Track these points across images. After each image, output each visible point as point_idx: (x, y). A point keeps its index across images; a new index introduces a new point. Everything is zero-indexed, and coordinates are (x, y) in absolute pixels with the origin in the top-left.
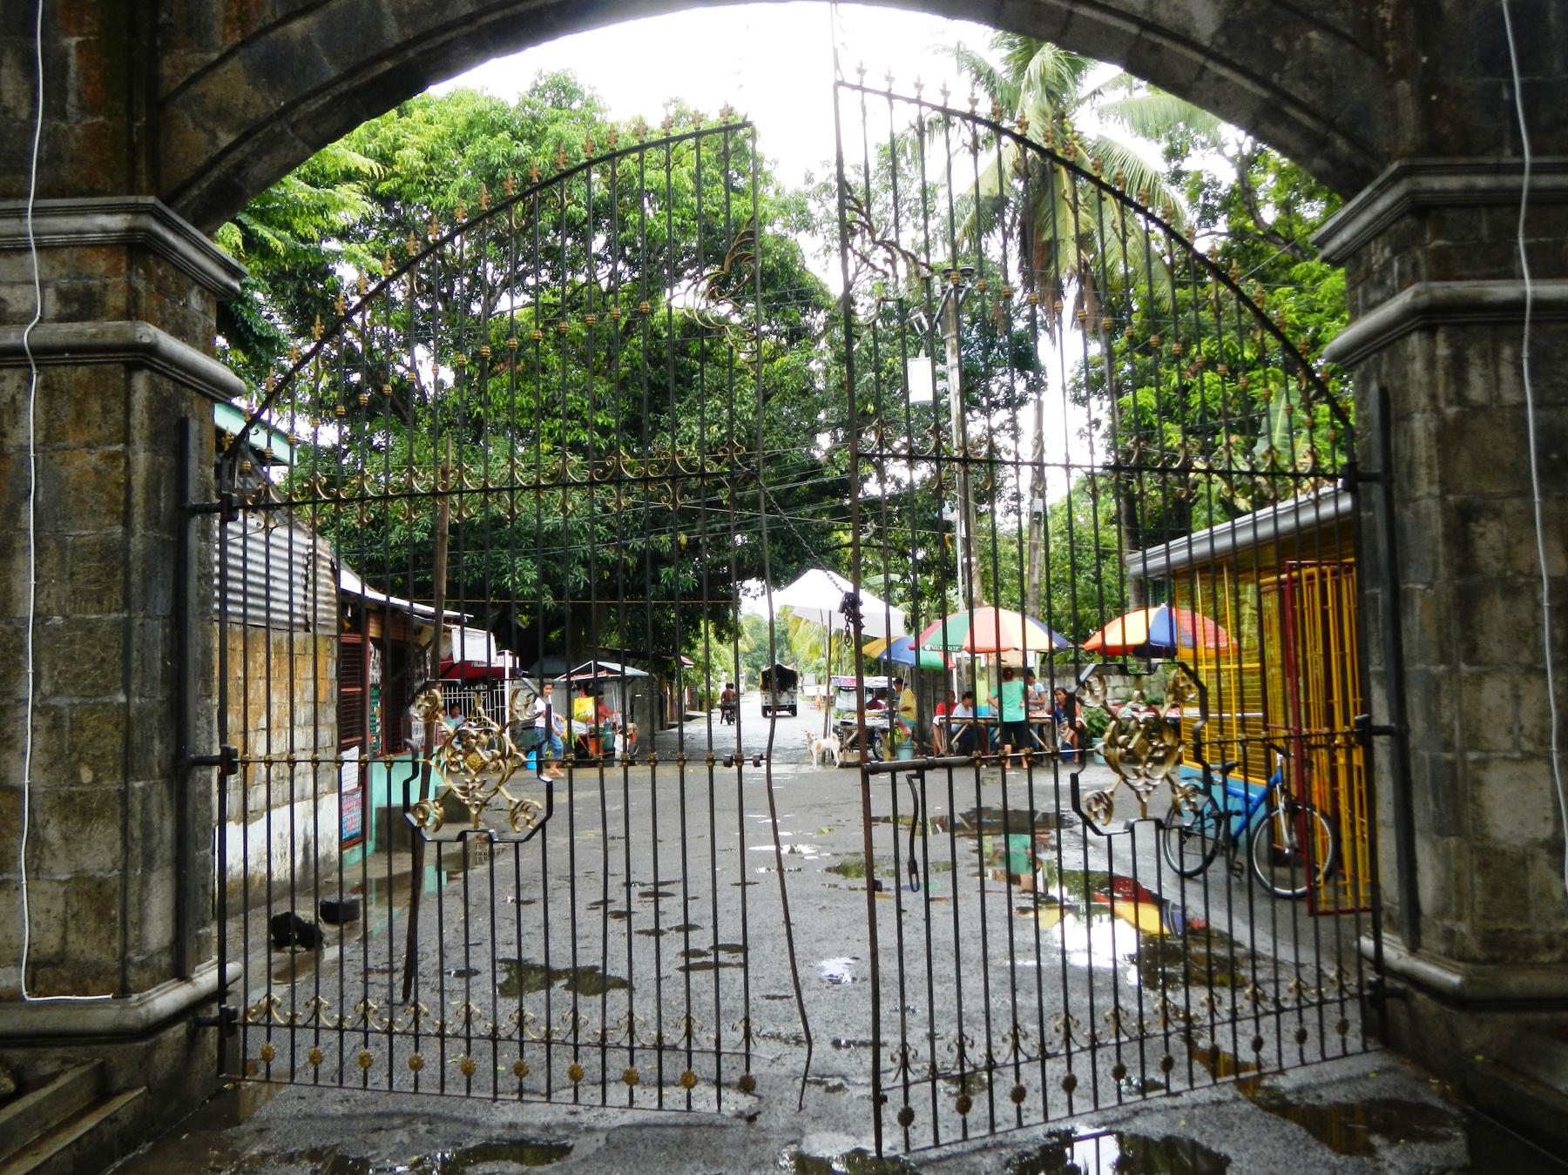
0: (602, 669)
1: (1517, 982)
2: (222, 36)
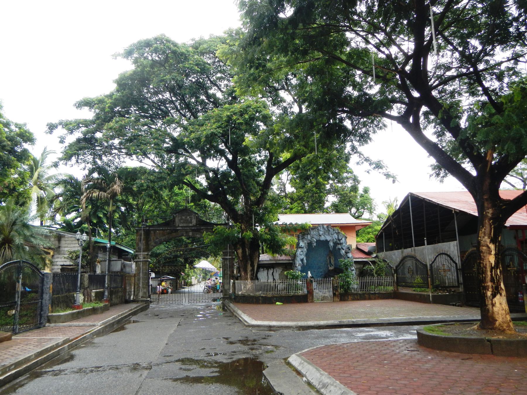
0: (166, 277)
1: (225, 297)
2: (152, 241)
